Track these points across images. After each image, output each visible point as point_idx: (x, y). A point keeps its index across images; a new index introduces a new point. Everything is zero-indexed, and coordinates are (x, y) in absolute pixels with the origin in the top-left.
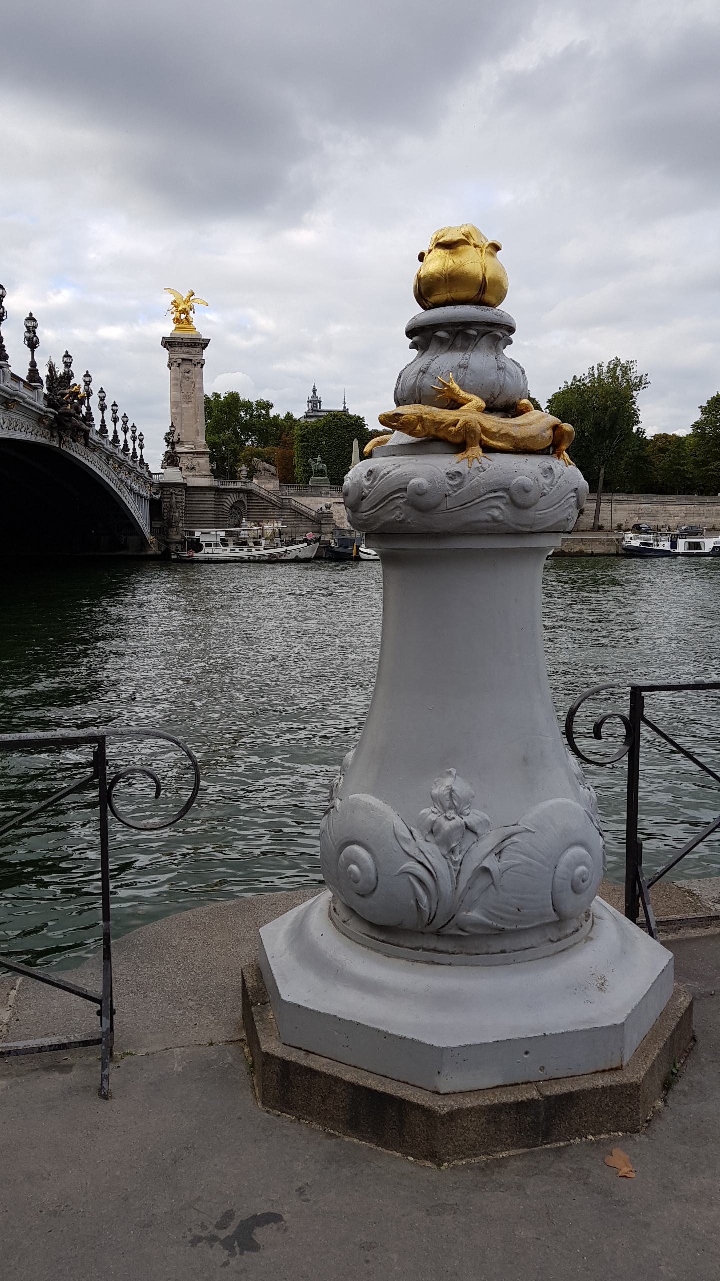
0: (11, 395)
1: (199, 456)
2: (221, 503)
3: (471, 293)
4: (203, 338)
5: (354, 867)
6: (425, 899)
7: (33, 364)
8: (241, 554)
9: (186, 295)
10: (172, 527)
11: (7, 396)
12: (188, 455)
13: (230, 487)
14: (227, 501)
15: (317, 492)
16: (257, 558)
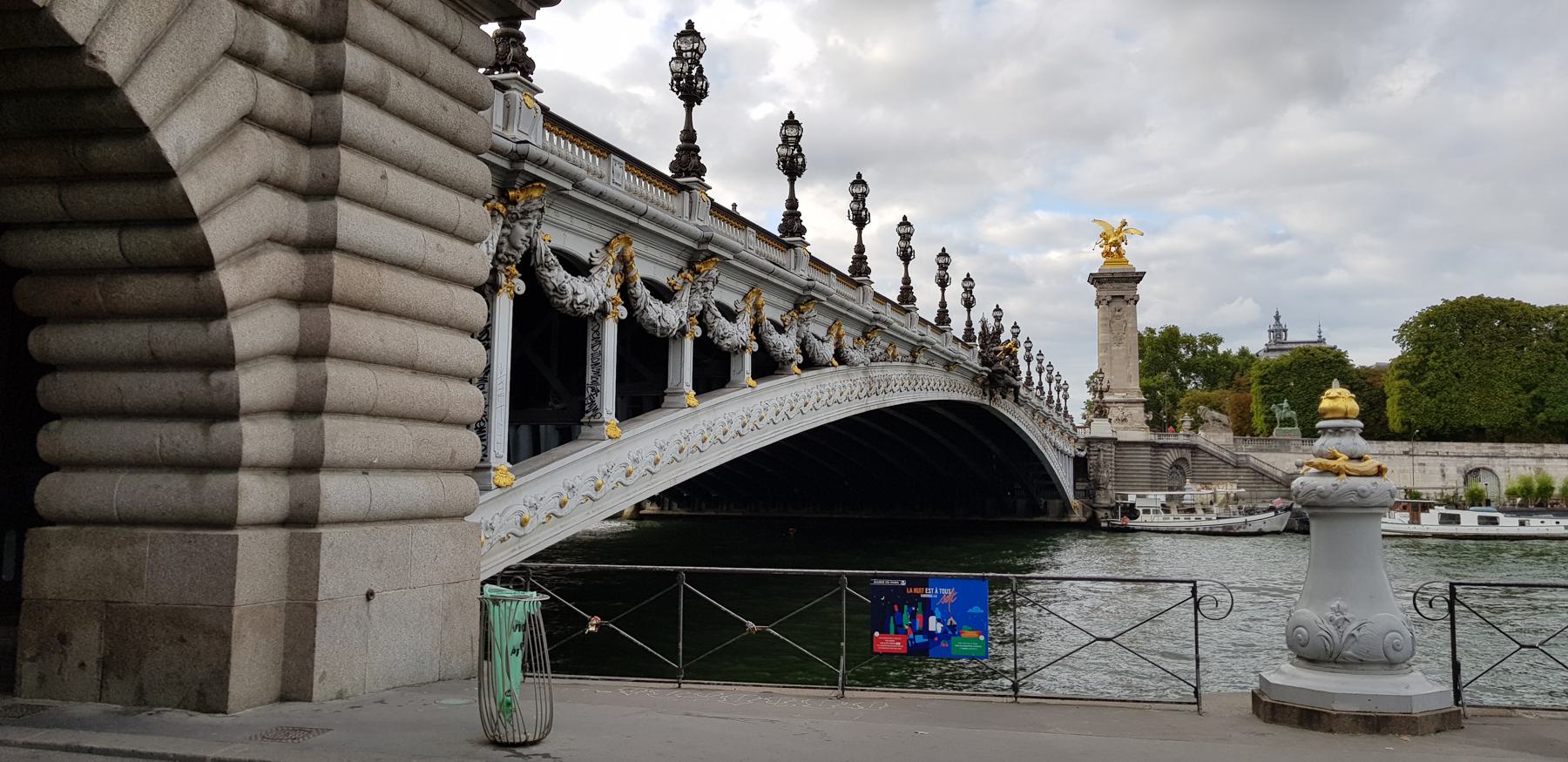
0: (953, 358)
1: (1131, 405)
2: (1157, 461)
3: (1342, 415)
4: (1137, 271)
5: (1300, 635)
6: (1328, 645)
7: (969, 323)
8: (1188, 524)
9: (1117, 225)
10: (1099, 489)
11: (949, 359)
12: (1117, 405)
13: (1169, 441)
14: (1165, 458)
15: (1283, 446)
16: (1208, 529)
